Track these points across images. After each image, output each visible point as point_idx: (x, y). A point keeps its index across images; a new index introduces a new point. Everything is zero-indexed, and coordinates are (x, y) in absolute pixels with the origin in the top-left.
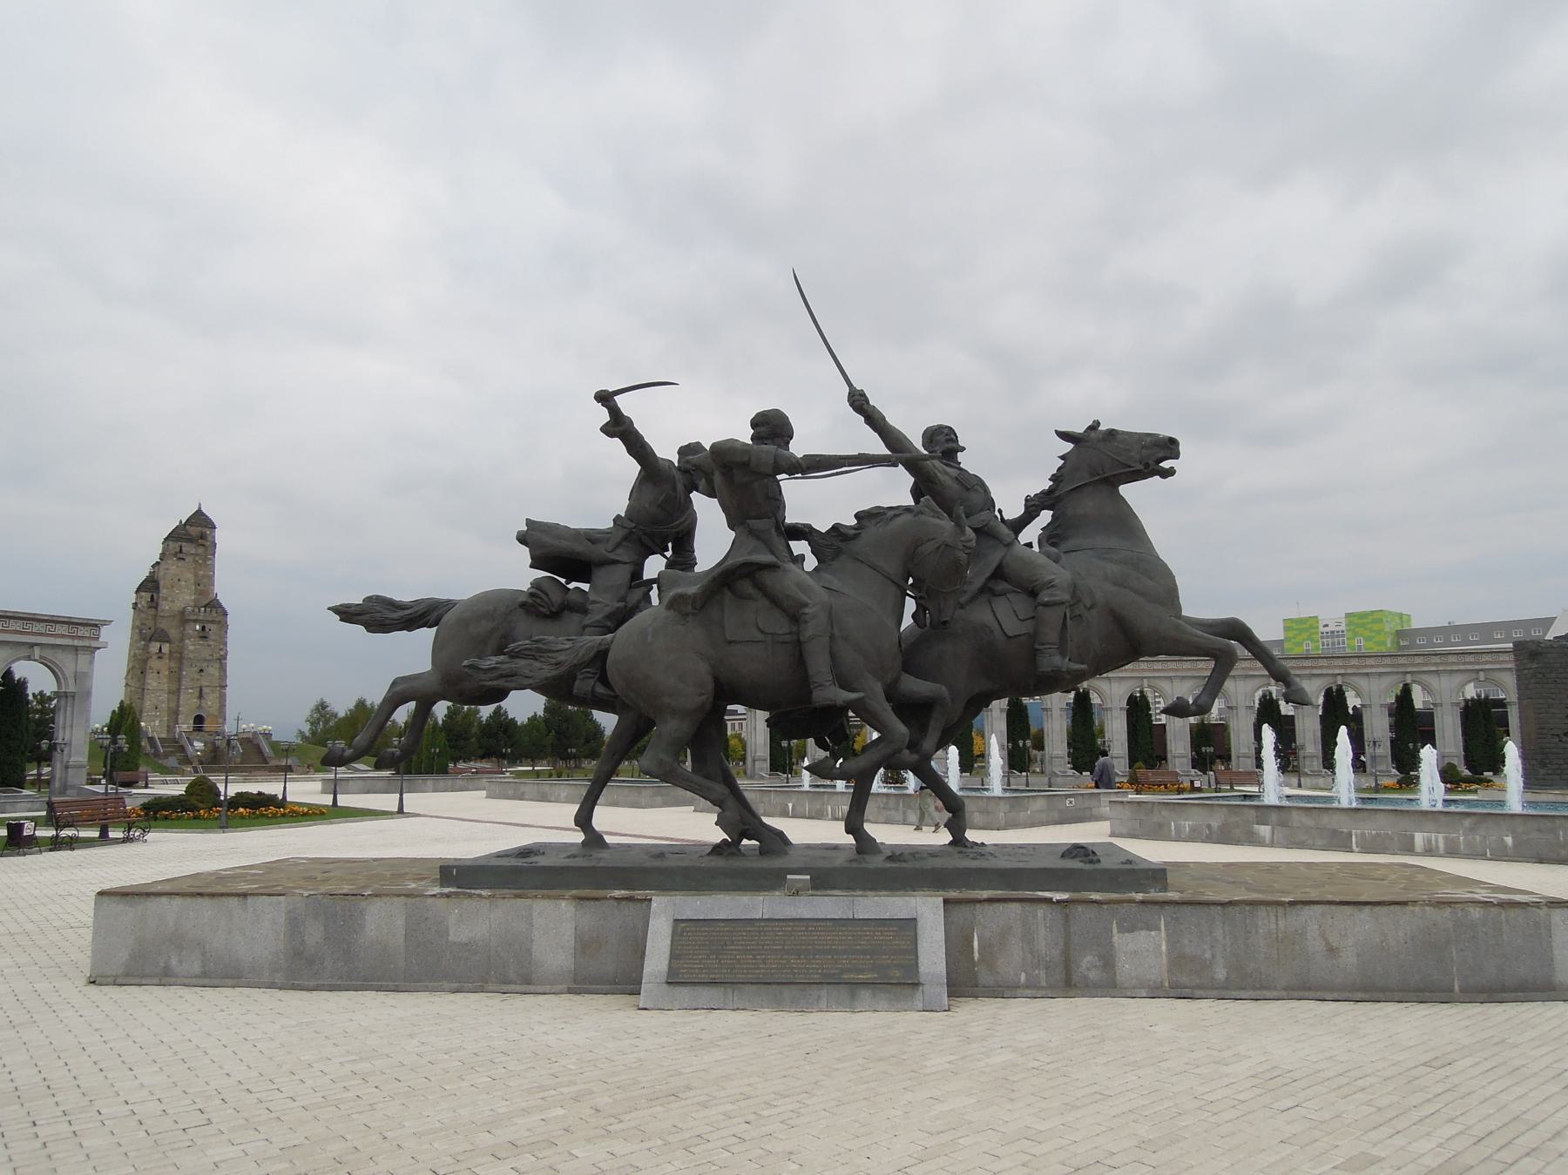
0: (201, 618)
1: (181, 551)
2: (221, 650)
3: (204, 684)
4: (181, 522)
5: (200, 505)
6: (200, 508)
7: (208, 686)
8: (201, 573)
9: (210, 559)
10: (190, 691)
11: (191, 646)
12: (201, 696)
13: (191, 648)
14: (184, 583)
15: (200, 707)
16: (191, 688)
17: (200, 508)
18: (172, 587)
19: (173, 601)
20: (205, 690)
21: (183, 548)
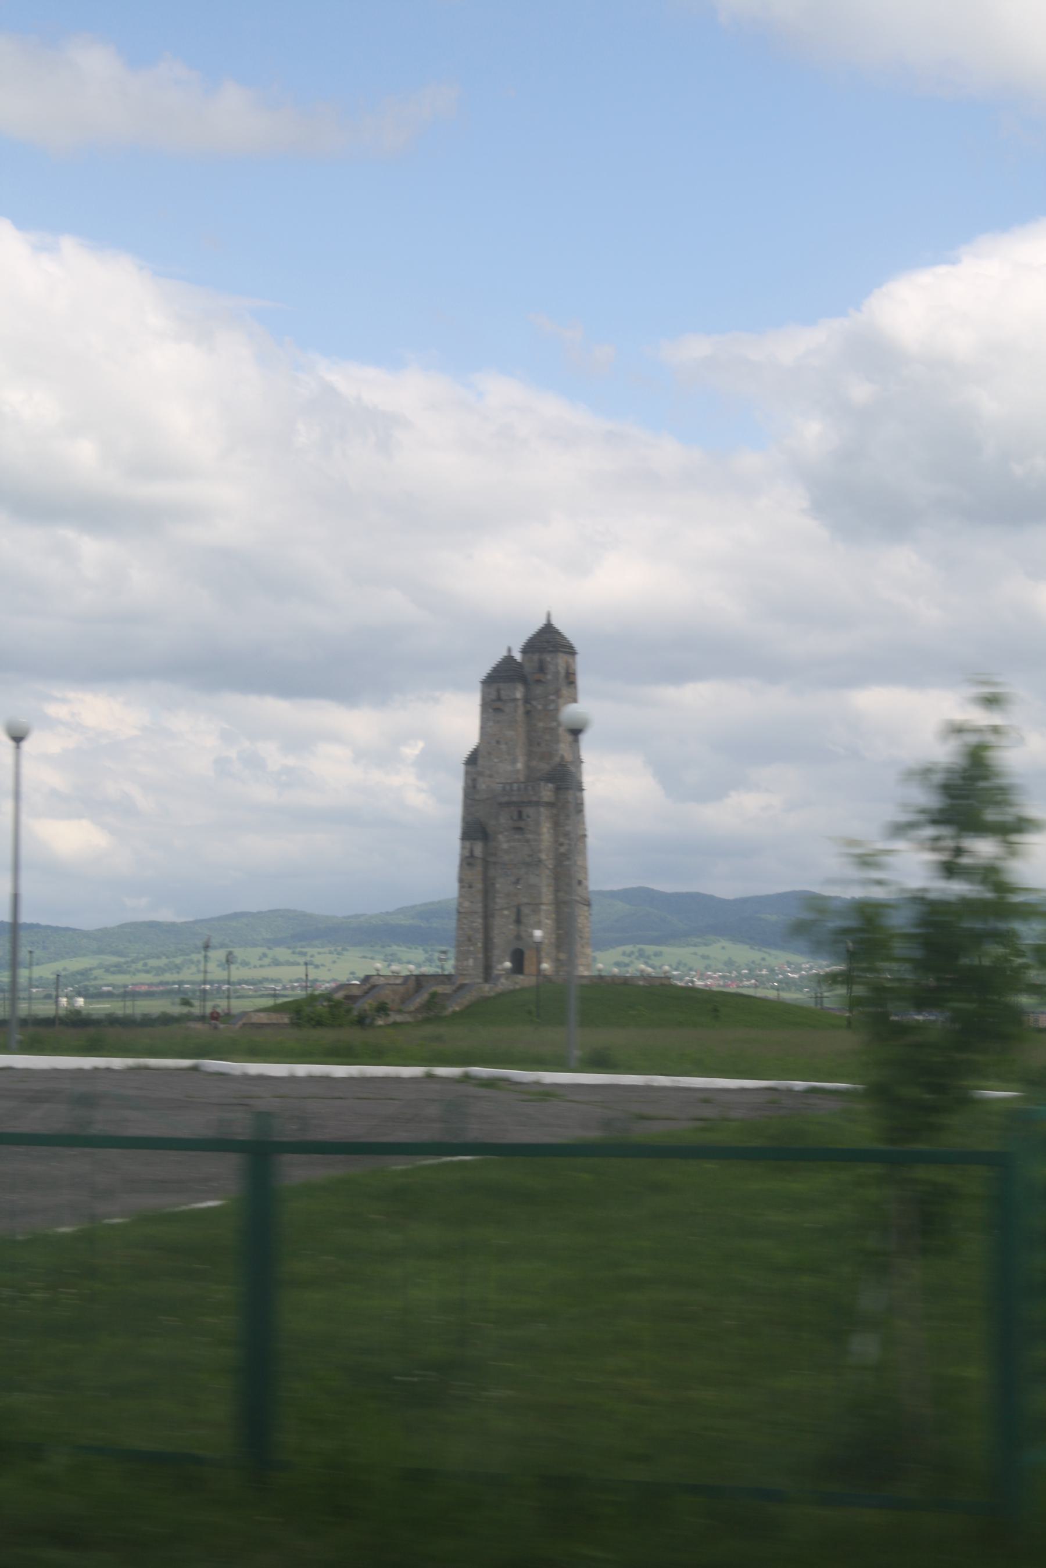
0: (514, 799)
1: (499, 699)
2: (561, 845)
3: (525, 900)
4: (509, 650)
5: (549, 615)
6: (549, 620)
7: (529, 904)
8: (541, 725)
9: (553, 701)
10: (506, 912)
11: (503, 842)
12: (518, 921)
13: (505, 846)
14: (503, 747)
15: (518, 937)
16: (506, 909)
17: (549, 620)
18: (489, 754)
19: (491, 776)
20: (526, 910)
21: (502, 692)
